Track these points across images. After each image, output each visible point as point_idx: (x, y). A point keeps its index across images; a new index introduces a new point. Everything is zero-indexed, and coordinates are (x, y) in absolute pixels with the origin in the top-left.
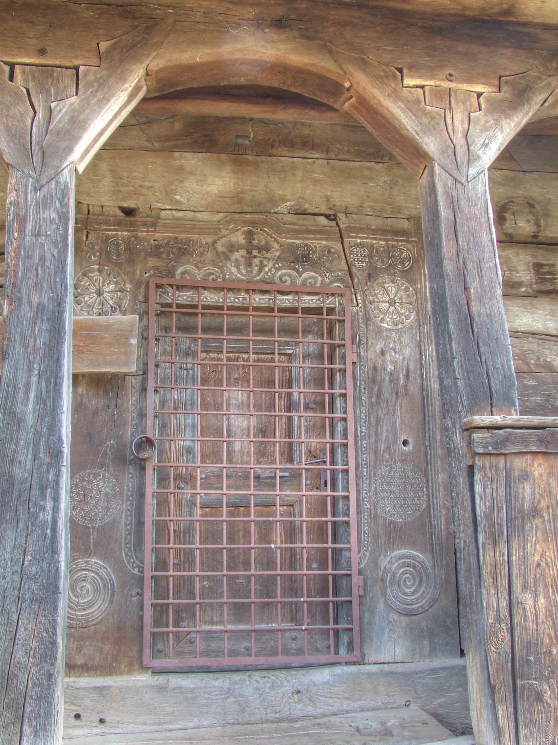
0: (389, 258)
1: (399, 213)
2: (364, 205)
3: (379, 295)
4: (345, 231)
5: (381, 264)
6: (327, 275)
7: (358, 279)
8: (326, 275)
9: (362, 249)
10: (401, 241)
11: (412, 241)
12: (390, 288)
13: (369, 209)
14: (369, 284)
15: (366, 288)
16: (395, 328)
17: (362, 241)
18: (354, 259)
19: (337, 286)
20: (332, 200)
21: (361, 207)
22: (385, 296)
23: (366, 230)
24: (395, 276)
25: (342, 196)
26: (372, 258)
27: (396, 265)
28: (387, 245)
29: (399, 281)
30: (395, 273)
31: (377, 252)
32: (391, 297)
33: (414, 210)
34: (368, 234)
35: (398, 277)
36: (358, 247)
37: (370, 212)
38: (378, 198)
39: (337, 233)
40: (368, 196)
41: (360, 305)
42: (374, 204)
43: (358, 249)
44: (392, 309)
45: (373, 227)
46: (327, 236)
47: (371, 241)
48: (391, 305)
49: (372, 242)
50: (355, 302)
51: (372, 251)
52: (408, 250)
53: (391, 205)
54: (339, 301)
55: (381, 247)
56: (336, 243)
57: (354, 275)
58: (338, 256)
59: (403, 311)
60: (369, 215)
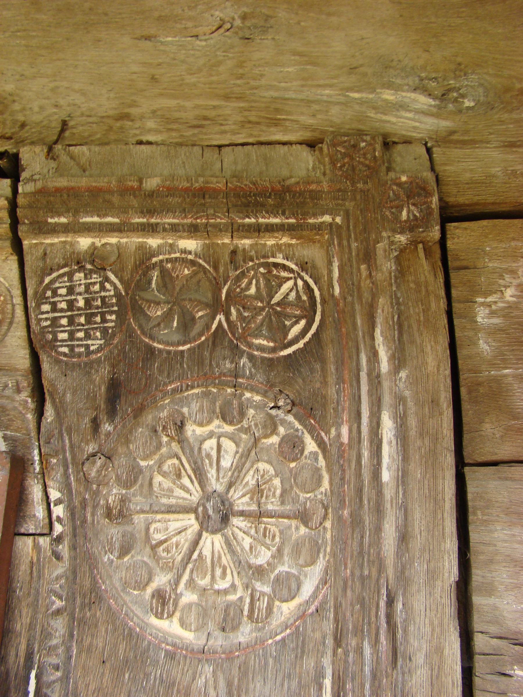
1: (276, 123)
2: (133, 111)
3: (158, 479)
4: (30, 206)
5: (176, 338)
9: (95, 278)
10: (270, 229)
11: (319, 228)
13: (151, 124)
14: (107, 427)
15: (91, 448)
17: (98, 242)
18: (55, 320)
20: (17, 107)
21: (126, 117)
22: (186, 481)
23: (116, 199)
25: (53, 90)
27: (243, 338)
29: (258, 407)
32: (220, 488)
33: (335, 110)
34: (123, 210)
35: (252, 389)
36: (82, 268)
37: (157, 131)
38: (191, 79)
40: (153, 79)
41: (58, 528)
42: (172, 103)
47: (136, 240)
49: (141, 247)
50: (40, 512)
52: (303, 266)
53: (239, 98)
55: (184, 261)
60: (149, 143)
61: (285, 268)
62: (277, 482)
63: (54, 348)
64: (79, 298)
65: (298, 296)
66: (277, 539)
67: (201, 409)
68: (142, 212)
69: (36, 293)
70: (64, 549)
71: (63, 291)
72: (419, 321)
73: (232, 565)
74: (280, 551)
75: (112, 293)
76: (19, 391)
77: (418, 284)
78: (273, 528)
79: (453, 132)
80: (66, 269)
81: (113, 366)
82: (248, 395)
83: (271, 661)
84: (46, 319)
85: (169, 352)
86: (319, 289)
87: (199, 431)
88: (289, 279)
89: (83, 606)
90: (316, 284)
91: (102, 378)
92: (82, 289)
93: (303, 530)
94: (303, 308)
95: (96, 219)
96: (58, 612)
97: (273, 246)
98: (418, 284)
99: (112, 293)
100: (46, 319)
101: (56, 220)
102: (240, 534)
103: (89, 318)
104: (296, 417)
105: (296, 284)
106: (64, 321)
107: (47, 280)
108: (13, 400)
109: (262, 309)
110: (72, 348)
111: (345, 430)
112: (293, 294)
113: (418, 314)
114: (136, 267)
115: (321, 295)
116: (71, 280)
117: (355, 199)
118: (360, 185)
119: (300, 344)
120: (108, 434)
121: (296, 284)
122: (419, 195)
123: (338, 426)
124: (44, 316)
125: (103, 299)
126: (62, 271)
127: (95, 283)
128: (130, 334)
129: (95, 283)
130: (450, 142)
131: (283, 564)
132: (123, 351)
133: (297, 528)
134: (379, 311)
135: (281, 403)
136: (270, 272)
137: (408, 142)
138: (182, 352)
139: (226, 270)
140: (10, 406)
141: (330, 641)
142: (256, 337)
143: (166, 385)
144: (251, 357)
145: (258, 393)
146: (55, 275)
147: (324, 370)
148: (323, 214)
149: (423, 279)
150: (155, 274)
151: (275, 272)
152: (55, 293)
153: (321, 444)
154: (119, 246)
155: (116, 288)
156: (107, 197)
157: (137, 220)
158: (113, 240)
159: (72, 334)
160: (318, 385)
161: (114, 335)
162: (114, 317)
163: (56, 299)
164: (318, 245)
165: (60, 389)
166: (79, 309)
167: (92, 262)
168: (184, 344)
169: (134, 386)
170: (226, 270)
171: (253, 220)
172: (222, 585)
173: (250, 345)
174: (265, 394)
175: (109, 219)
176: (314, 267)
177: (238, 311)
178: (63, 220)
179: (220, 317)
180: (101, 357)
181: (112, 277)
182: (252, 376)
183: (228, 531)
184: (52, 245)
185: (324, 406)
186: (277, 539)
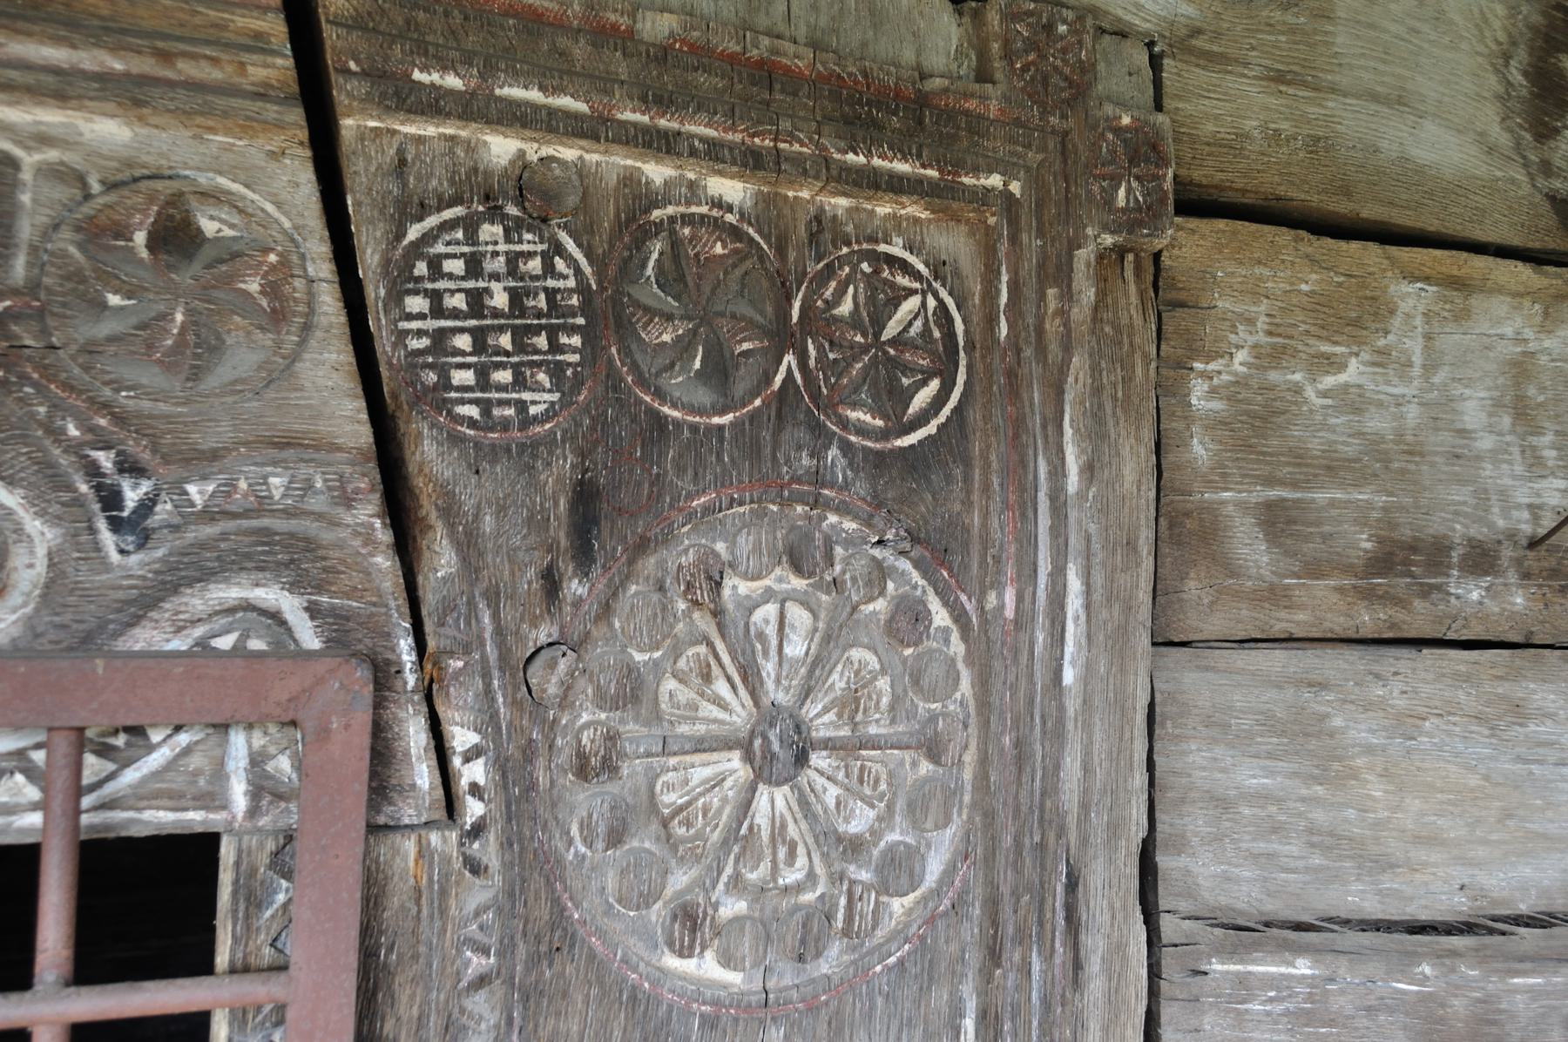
0: (782, 337)
5: (703, 396)
6: (132, 495)
7: (468, 545)
8: (111, 500)
9: (529, 242)
11: (983, 197)
12: (770, 610)
14: (575, 587)
15: (543, 634)
16: (786, 977)
17: (534, 152)
18: (440, 339)
19: (248, 606)
22: (722, 688)
23: (580, 51)
24: (816, 502)
26: (624, 330)
27: (830, 407)
28: (768, 212)
30: (818, 478)
31: (673, 276)
32: (778, 694)
34: (601, 83)
35: (843, 510)
36: (495, 214)
39: (258, 44)
41: (474, 809)
43: (490, 231)
44: (772, 802)
45: (657, 26)
46: (144, 65)
47: (620, 161)
48: (764, 770)
49: (630, 180)
50: (424, 775)
51: (630, 268)
54: (257, 761)
55: (717, 224)
56: (251, 149)
57: (428, 508)
58: (272, 290)
59: (860, 821)
61: (905, 267)
62: (883, 684)
63: (444, 406)
64: (496, 287)
65: (926, 329)
66: (883, 787)
67: (757, 549)
68: (644, 99)
69: (386, 263)
70: (488, 850)
71: (456, 266)
72: (1115, 398)
73: (810, 841)
74: (890, 808)
75: (571, 283)
76: (348, 501)
77: (1118, 329)
78: (875, 767)
79: (1196, 32)
80: (458, 211)
81: (582, 454)
82: (833, 518)
83: (880, 1001)
84: (420, 333)
85: (694, 428)
86: (965, 321)
87: (744, 587)
88: (913, 292)
89: (534, 961)
90: (959, 309)
91: (560, 480)
92: (499, 265)
93: (925, 767)
94: (933, 354)
95: (534, 95)
96: (482, 981)
97: (887, 217)
98: (1118, 329)
99: (571, 283)
100: (420, 333)
101: (435, 77)
102: (820, 781)
103: (520, 334)
104: (917, 565)
105: (924, 304)
106: (463, 342)
107: (414, 232)
108: (335, 523)
109: (865, 349)
110: (486, 406)
111: (1010, 596)
112: (918, 324)
113: (1115, 385)
114: (620, 226)
115: (966, 332)
116: (472, 238)
117: (1043, 148)
118: (1054, 120)
119: (931, 429)
120: (578, 603)
121: (924, 304)
122: (1147, 161)
123: (999, 586)
124: (415, 325)
125: (551, 294)
126: (448, 214)
127: (530, 255)
128: (613, 381)
129: (530, 255)
130: (1191, 51)
131: (893, 830)
132: (599, 421)
133: (914, 764)
134: (1071, 379)
135: (889, 536)
136: (877, 272)
137: (1122, 34)
138: (721, 428)
139: (801, 259)
140: (327, 536)
141: (974, 958)
142: (854, 406)
143: (690, 497)
144: (846, 448)
145: (855, 518)
146: (432, 221)
147: (967, 479)
148: (991, 172)
149: (1125, 321)
150: (656, 248)
151: (886, 274)
152: (435, 264)
153: (959, 616)
154: (580, 169)
155: (578, 271)
156: (563, 42)
157: (628, 116)
158: (568, 153)
159: (483, 373)
160: (957, 507)
161: (578, 382)
162: (576, 341)
163: (441, 285)
164: (963, 228)
165: (469, 505)
166: (496, 313)
167: (520, 200)
168: (722, 413)
169: (624, 497)
170: (801, 259)
171: (862, 159)
172: (791, 877)
173: (844, 423)
174: (868, 522)
175: (565, 102)
176: (957, 273)
177: (820, 348)
178: (453, 81)
179: (789, 359)
180: (552, 432)
181: (570, 245)
182: (846, 486)
183: (802, 780)
184: (420, 140)
185: (966, 545)
186: (883, 787)
